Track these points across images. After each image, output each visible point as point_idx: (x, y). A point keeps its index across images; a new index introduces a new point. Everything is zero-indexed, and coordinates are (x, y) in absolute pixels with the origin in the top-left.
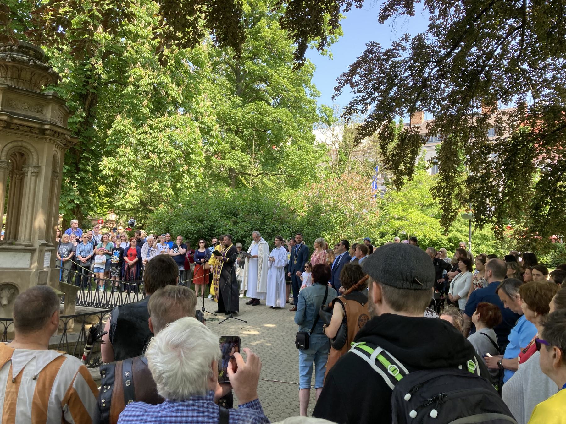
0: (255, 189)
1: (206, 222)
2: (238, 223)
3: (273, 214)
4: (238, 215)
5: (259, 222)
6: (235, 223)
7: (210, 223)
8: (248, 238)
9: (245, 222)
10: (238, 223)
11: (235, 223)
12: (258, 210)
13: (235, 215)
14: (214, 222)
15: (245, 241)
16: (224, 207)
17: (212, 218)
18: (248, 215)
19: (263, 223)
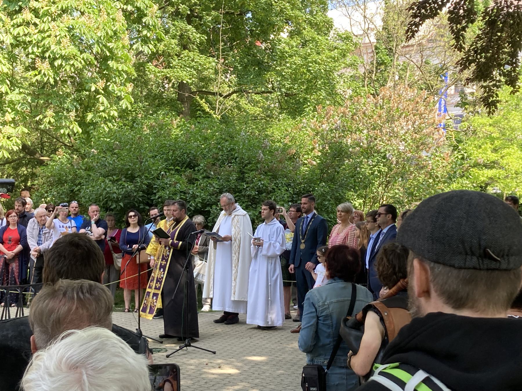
0: (225, 120)
2: (197, 180)
3: (259, 162)
5: (234, 176)
6: (191, 181)
7: (145, 182)
8: (214, 207)
9: (208, 177)
10: (197, 180)
11: (191, 181)
12: (231, 157)
13: (191, 165)
15: (209, 212)
16: (171, 153)
17: (149, 173)
18: (214, 165)
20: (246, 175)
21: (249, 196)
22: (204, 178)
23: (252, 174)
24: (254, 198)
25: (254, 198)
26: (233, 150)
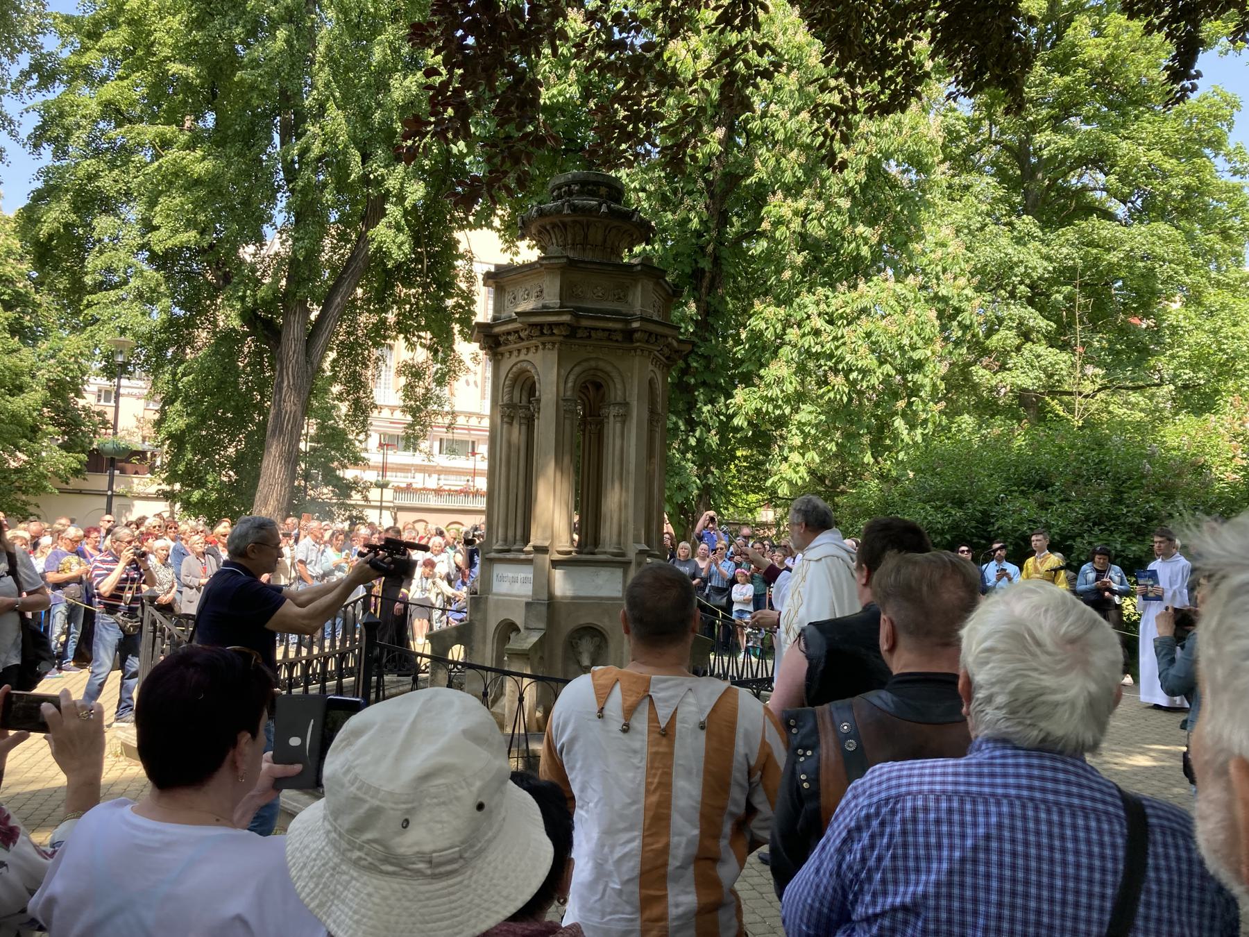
1: (970, 505)
2: (1051, 504)
3: (1144, 477)
4: (1047, 486)
5: (1107, 497)
6: (1043, 506)
7: (979, 508)
8: (1079, 540)
9: (1068, 500)
10: (1051, 504)
11: (1043, 506)
12: (1100, 471)
13: (1043, 484)
14: (990, 504)
15: (1071, 547)
16: (1013, 470)
17: (984, 496)
18: (1075, 483)
19: (1118, 500)
20: (1126, 495)
21: (1131, 524)
22: (1061, 501)
23: (1134, 494)
24: (1139, 527)
25: (1139, 527)
26: (1101, 461)
